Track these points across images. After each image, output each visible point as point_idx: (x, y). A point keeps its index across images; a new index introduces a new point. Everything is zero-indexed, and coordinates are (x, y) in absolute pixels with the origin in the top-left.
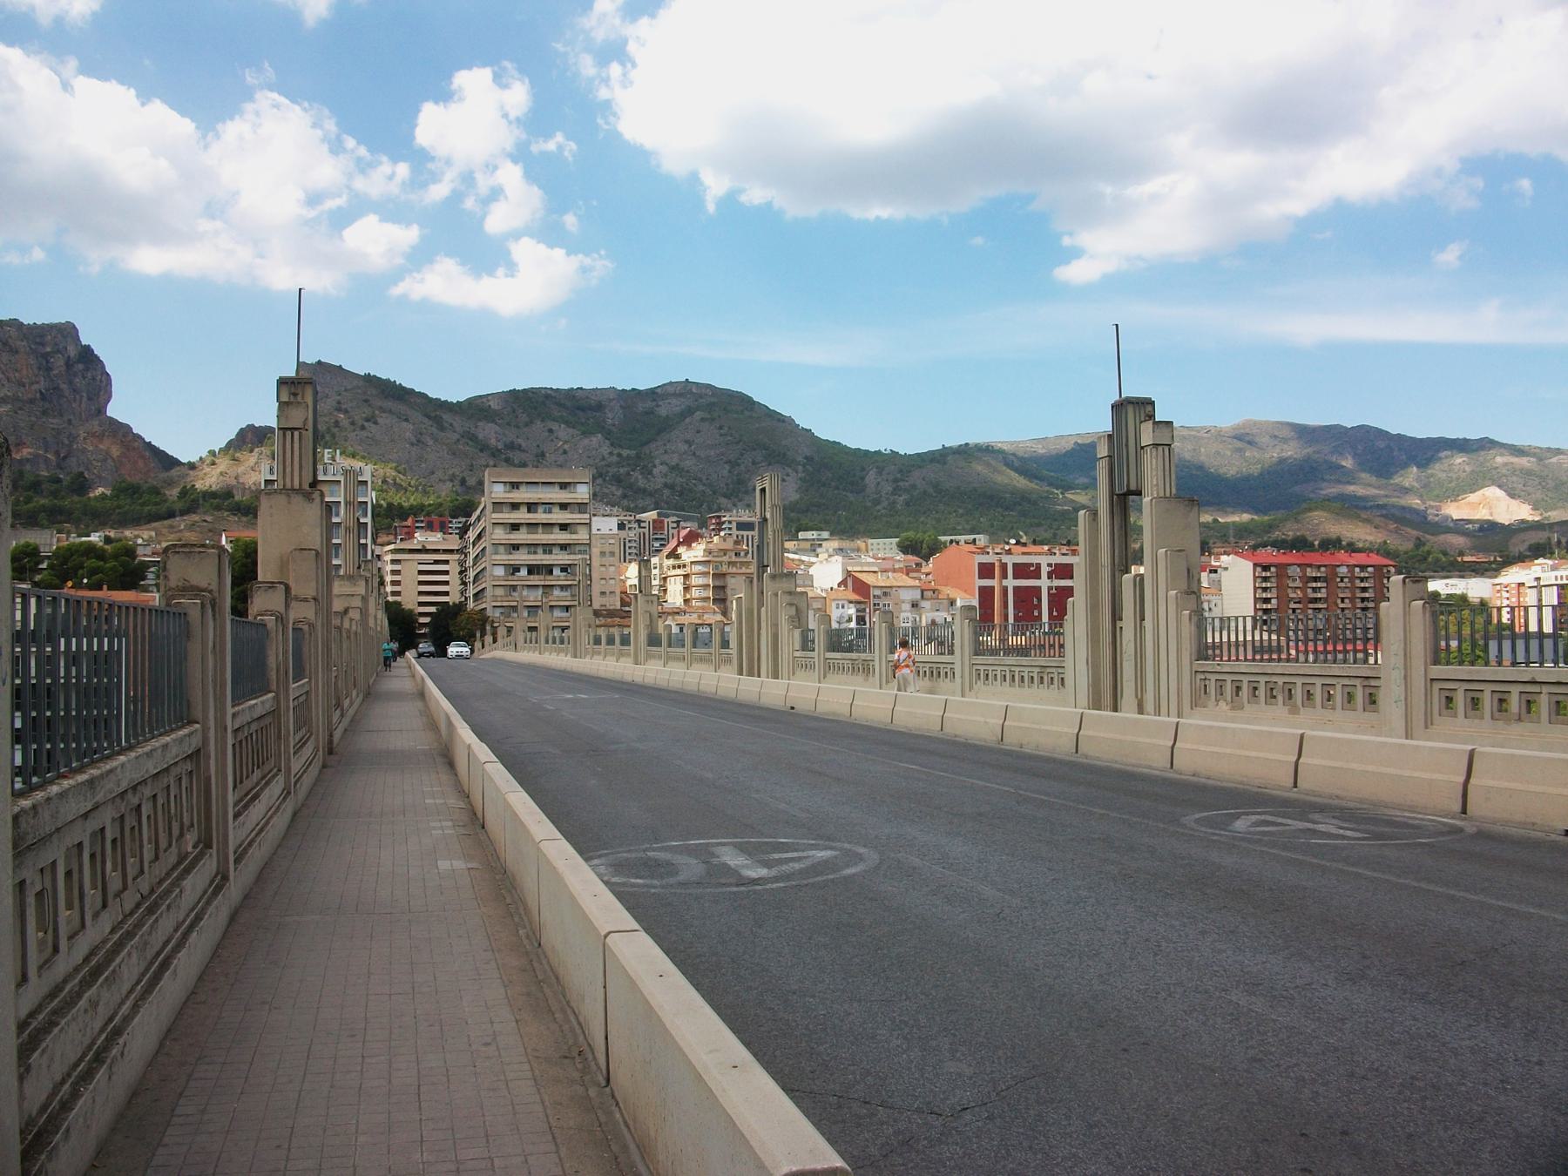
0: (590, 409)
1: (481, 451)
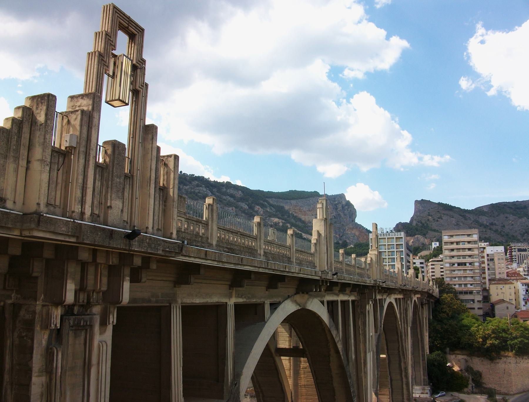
0: (521, 208)
1: (480, 226)
